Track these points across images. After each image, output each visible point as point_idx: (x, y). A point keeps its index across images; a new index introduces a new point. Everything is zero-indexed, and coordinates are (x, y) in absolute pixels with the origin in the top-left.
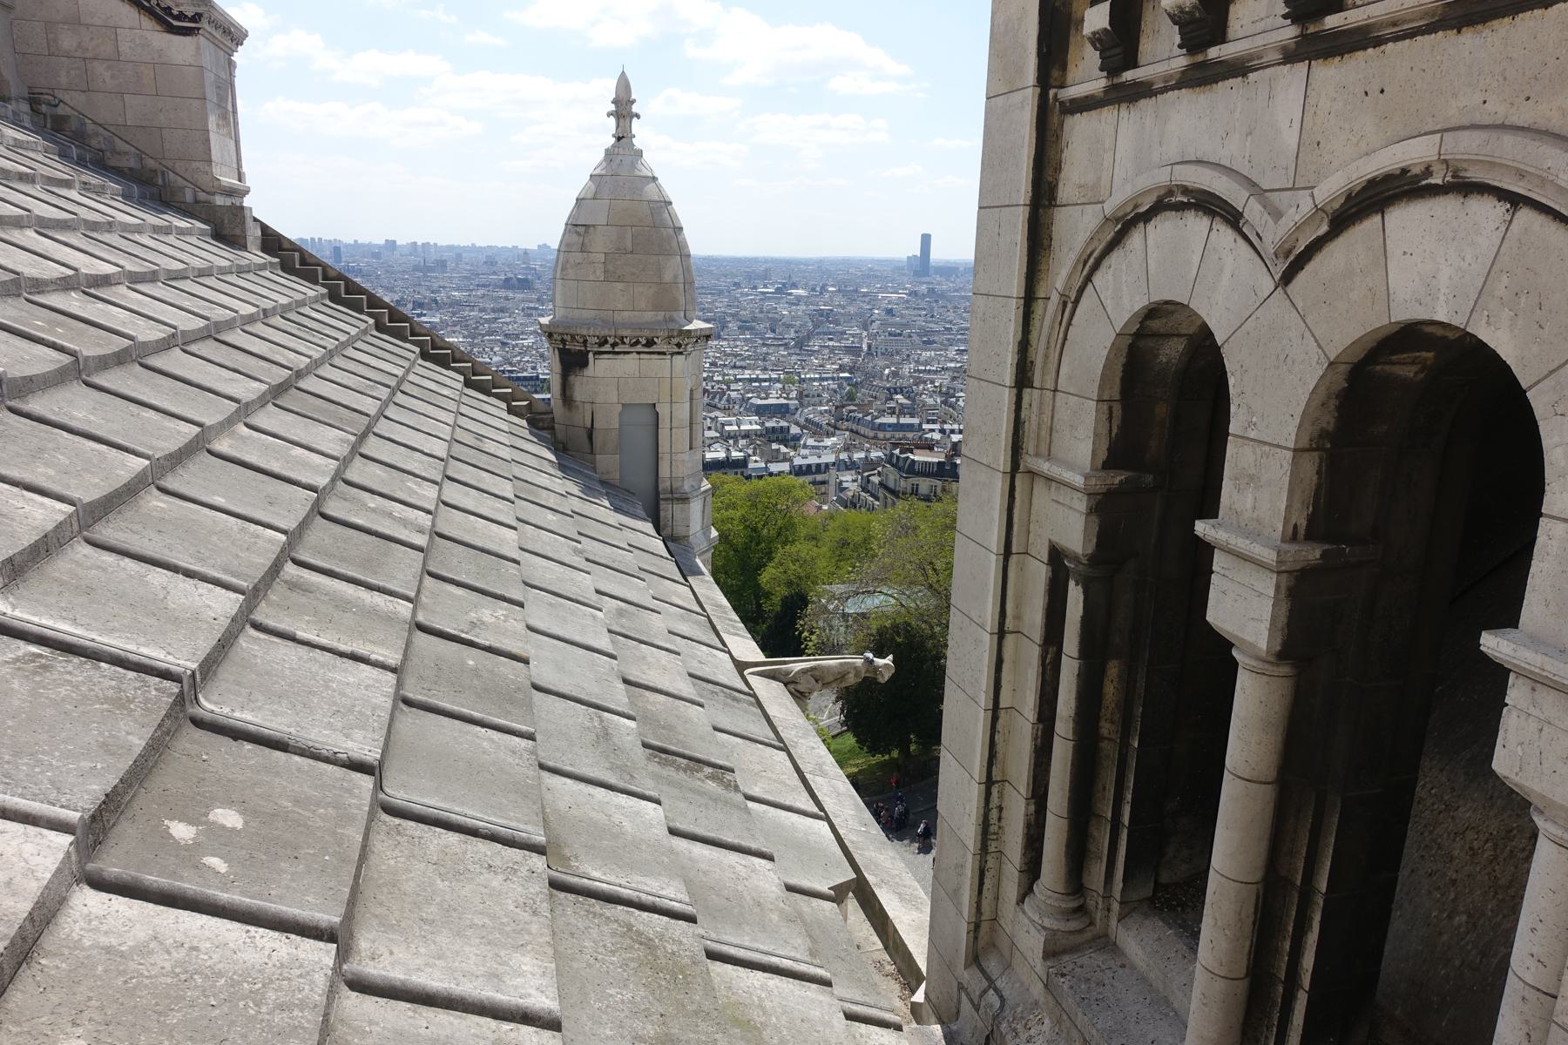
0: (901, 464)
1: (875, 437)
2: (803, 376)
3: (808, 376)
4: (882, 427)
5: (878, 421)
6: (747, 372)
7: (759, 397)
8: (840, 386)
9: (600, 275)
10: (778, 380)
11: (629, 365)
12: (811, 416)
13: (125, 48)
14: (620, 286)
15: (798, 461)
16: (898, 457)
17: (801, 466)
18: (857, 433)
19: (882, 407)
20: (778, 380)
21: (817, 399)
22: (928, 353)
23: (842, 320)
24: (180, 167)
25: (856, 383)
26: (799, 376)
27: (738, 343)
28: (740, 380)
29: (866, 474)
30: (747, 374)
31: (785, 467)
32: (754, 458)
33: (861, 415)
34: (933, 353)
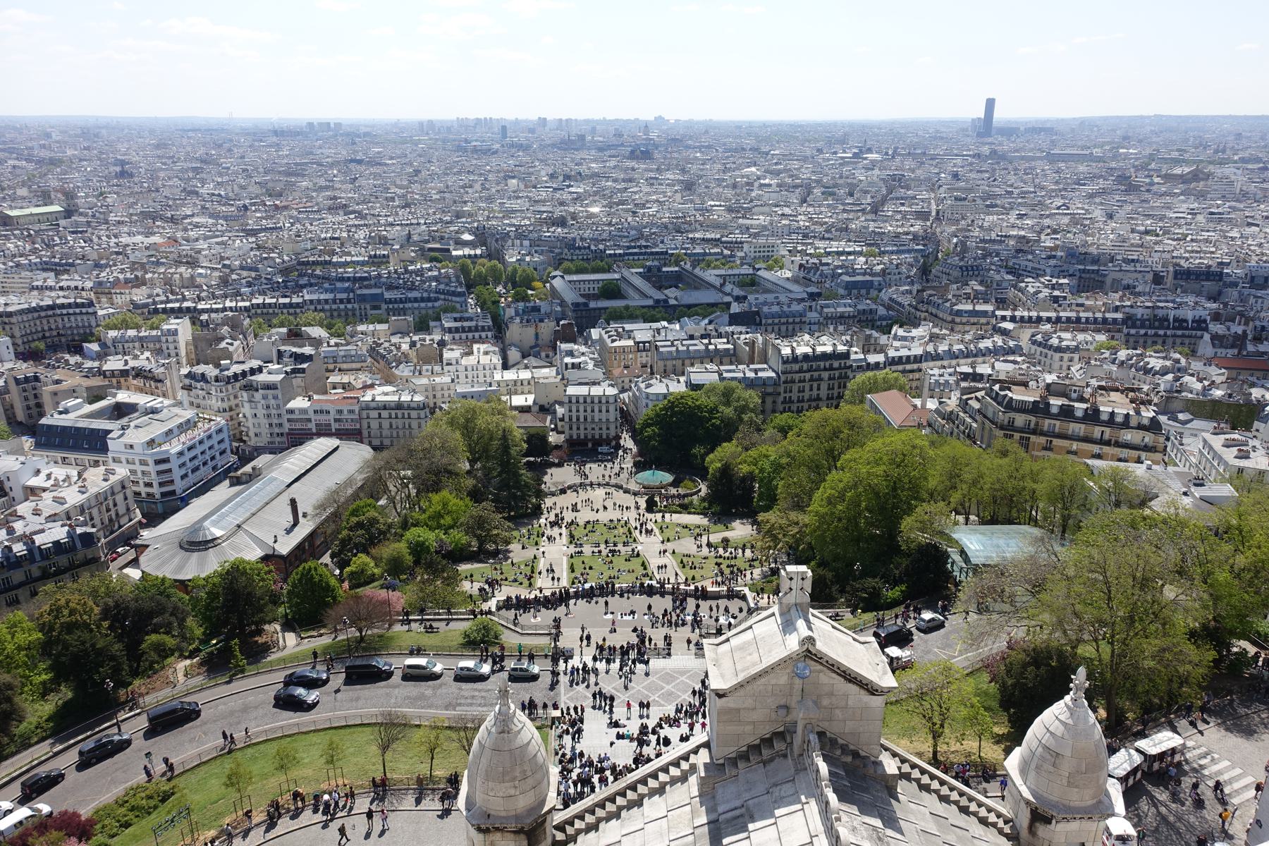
0: (1000, 399)
1: (953, 322)
4: (959, 313)
5: (956, 308)
7: (847, 274)
8: (916, 259)
9: (1065, 782)
10: (860, 253)
11: (1074, 825)
12: (895, 296)
13: (850, 703)
14: (1076, 790)
15: (892, 353)
16: (997, 393)
17: (893, 358)
18: (936, 316)
19: (958, 293)
20: (860, 253)
21: (898, 277)
22: (991, 217)
24: (865, 748)
27: (823, 209)
28: (829, 254)
29: (965, 397)
31: (880, 358)
32: (854, 349)
33: (940, 301)
34: (995, 217)
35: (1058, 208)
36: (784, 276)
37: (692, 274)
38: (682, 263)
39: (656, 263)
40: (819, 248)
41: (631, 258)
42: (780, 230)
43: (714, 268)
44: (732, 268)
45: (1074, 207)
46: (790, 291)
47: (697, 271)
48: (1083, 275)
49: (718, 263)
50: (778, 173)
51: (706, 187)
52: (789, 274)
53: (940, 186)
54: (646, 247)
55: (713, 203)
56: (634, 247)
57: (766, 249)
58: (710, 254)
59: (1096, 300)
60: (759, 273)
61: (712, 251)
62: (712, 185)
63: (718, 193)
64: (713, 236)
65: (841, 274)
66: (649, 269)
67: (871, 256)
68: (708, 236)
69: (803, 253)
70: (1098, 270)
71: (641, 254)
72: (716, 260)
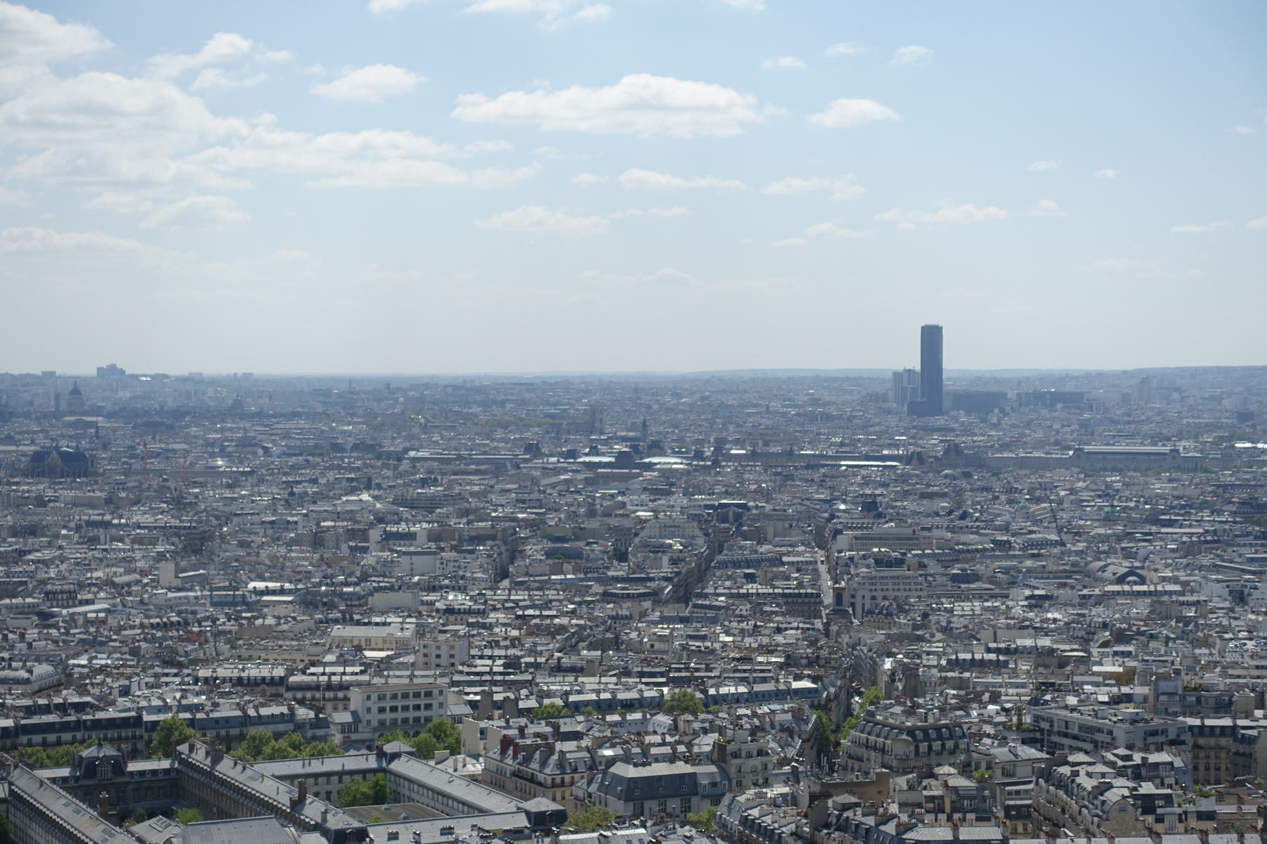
2: (712, 691)
3: (724, 690)
6: (590, 682)
7: (627, 759)
8: (798, 715)
10: (657, 705)
12: (755, 813)
19: (912, 797)
21: (757, 762)
22: (967, 606)
23: (770, 531)
25: (828, 700)
26: (705, 692)
27: (551, 594)
28: (577, 708)
30: (591, 688)
33: (870, 821)
35: (1121, 580)
36: (462, 772)
37: (210, 775)
38: (183, 748)
39: (109, 751)
40: (549, 694)
41: (37, 738)
42: (444, 651)
43: (271, 758)
44: (320, 755)
45: (1154, 576)
46: (482, 812)
47: (226, 768)
48: (1202, 741)
49: (282, 743)
50: (426, 506)
51: (243, 544)
52: (476, 767)
53: (838, 532)
54: (80, 707)
55: (261, 585)
56: (47, 710)
57: (411, 702)
58: (260, 720)
59: (1241, 801)
60: (396, 766)
61: (264, 711)
62: (259, 539)
63: (274, 558)
64: (265, 672)
65: (611, 761)
66: (90, 768)
67: (685, 710)
68: (253, 671)
69: (509, 708)
70: (1234, 728)
71: (65, 727)
72: (278, 736)
